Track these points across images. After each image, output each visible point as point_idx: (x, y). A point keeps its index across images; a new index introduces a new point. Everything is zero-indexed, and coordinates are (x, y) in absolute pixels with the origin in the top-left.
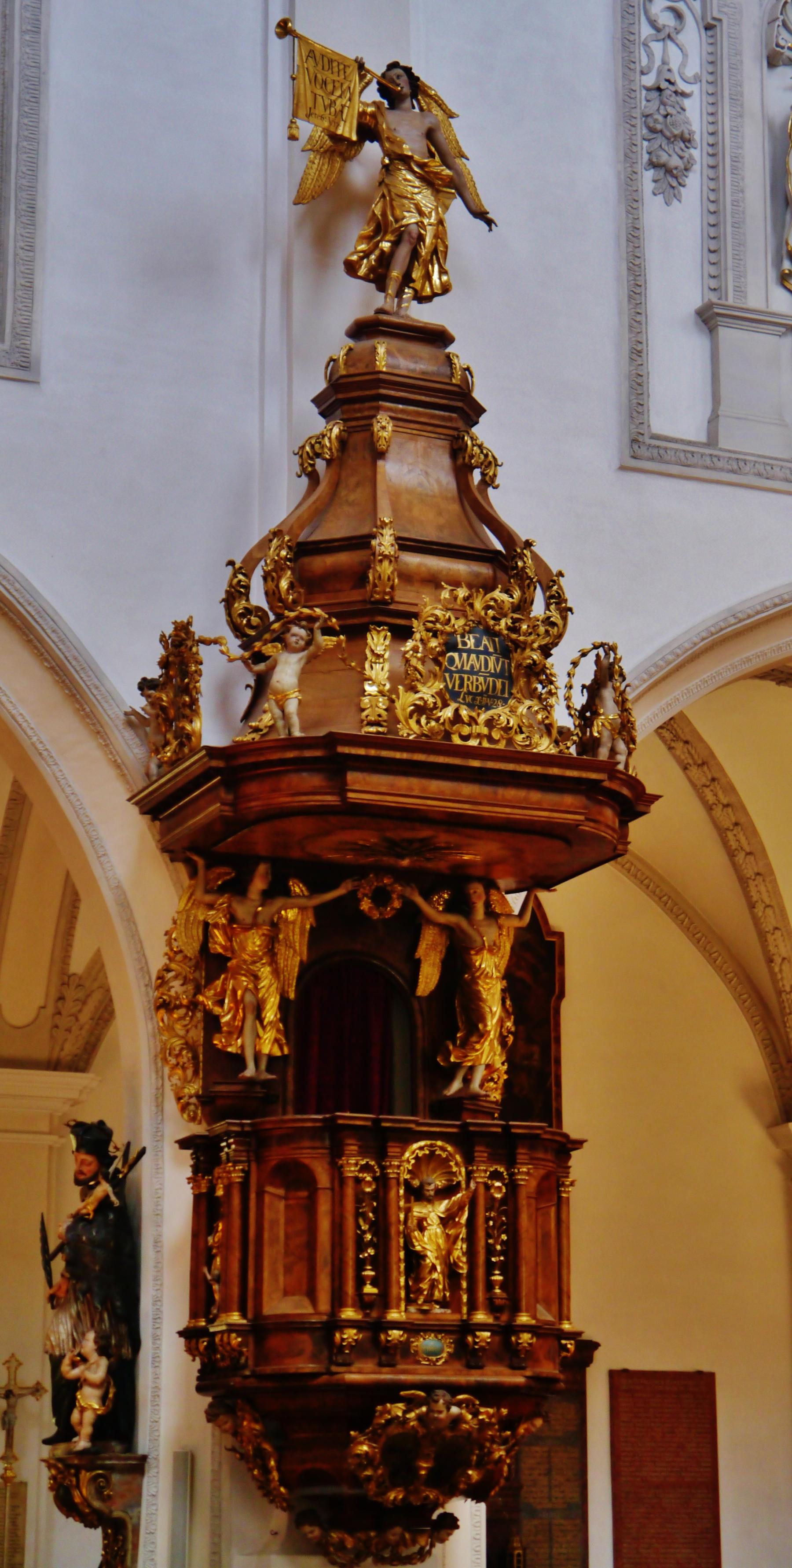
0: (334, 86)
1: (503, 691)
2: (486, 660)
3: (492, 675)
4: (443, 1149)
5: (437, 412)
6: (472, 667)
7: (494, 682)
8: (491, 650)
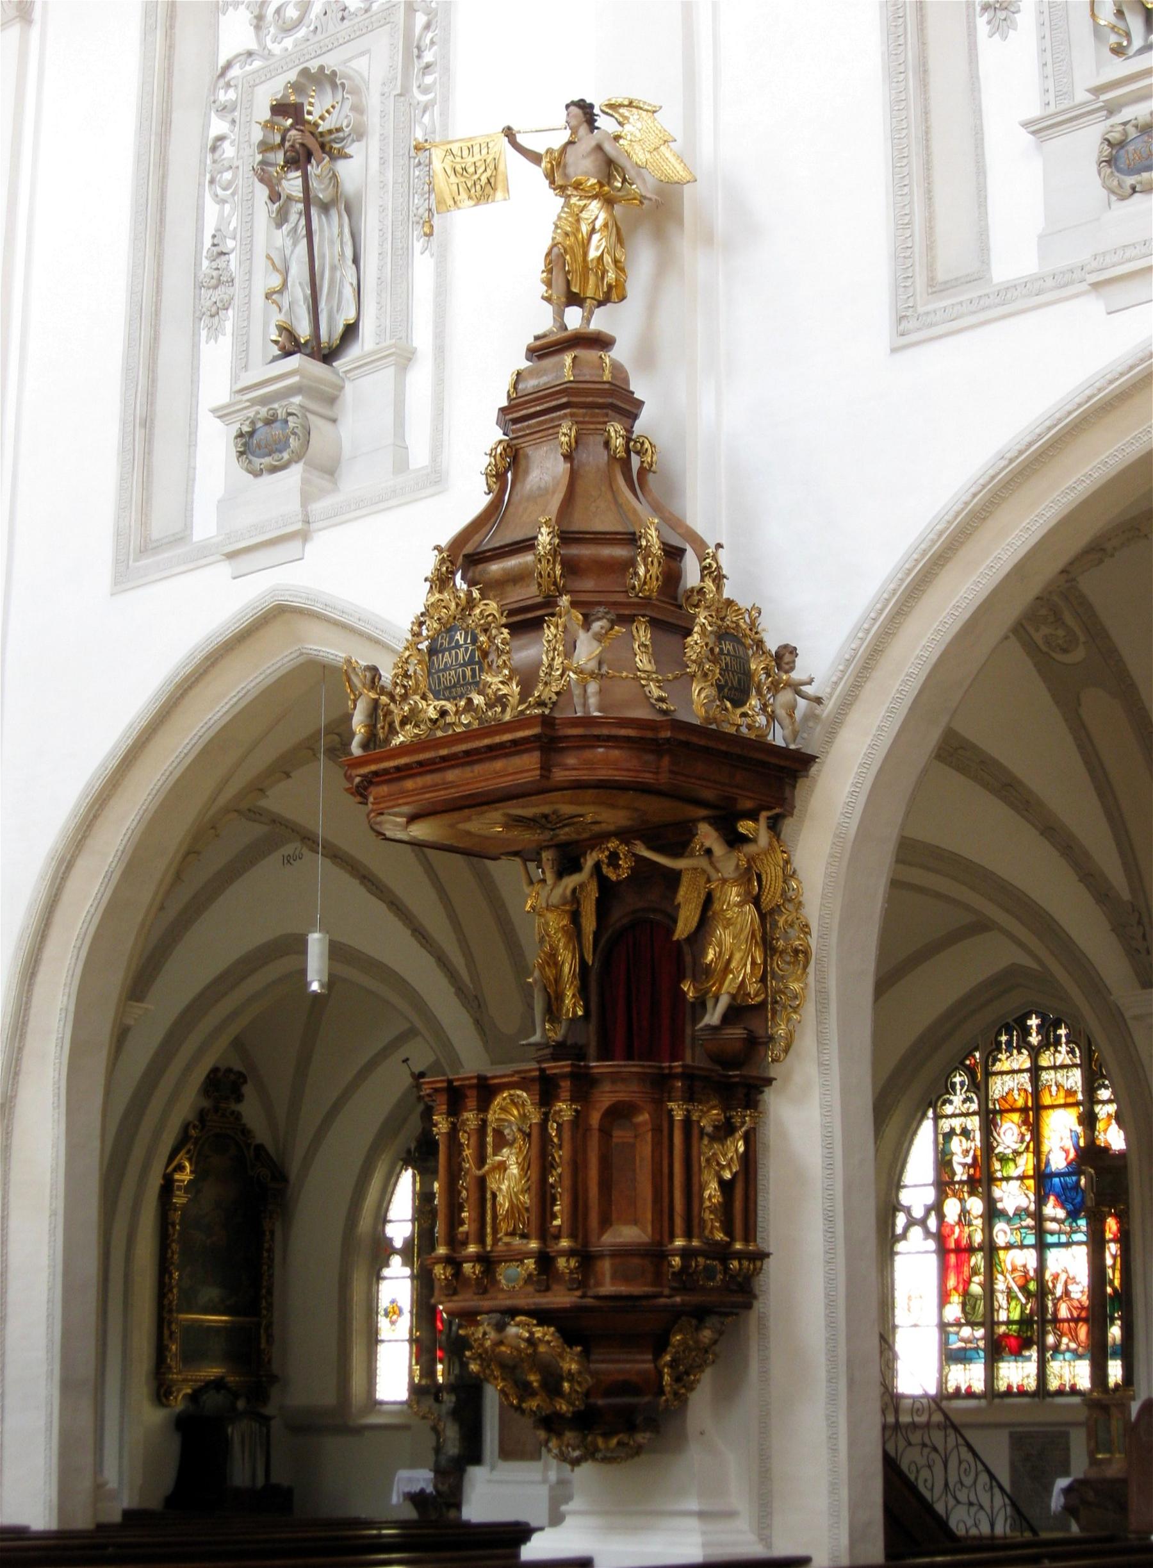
1: (474, 675)
2: (457, 654)
3: (461, 665)
7: (464, 672)
8: (461, 642)
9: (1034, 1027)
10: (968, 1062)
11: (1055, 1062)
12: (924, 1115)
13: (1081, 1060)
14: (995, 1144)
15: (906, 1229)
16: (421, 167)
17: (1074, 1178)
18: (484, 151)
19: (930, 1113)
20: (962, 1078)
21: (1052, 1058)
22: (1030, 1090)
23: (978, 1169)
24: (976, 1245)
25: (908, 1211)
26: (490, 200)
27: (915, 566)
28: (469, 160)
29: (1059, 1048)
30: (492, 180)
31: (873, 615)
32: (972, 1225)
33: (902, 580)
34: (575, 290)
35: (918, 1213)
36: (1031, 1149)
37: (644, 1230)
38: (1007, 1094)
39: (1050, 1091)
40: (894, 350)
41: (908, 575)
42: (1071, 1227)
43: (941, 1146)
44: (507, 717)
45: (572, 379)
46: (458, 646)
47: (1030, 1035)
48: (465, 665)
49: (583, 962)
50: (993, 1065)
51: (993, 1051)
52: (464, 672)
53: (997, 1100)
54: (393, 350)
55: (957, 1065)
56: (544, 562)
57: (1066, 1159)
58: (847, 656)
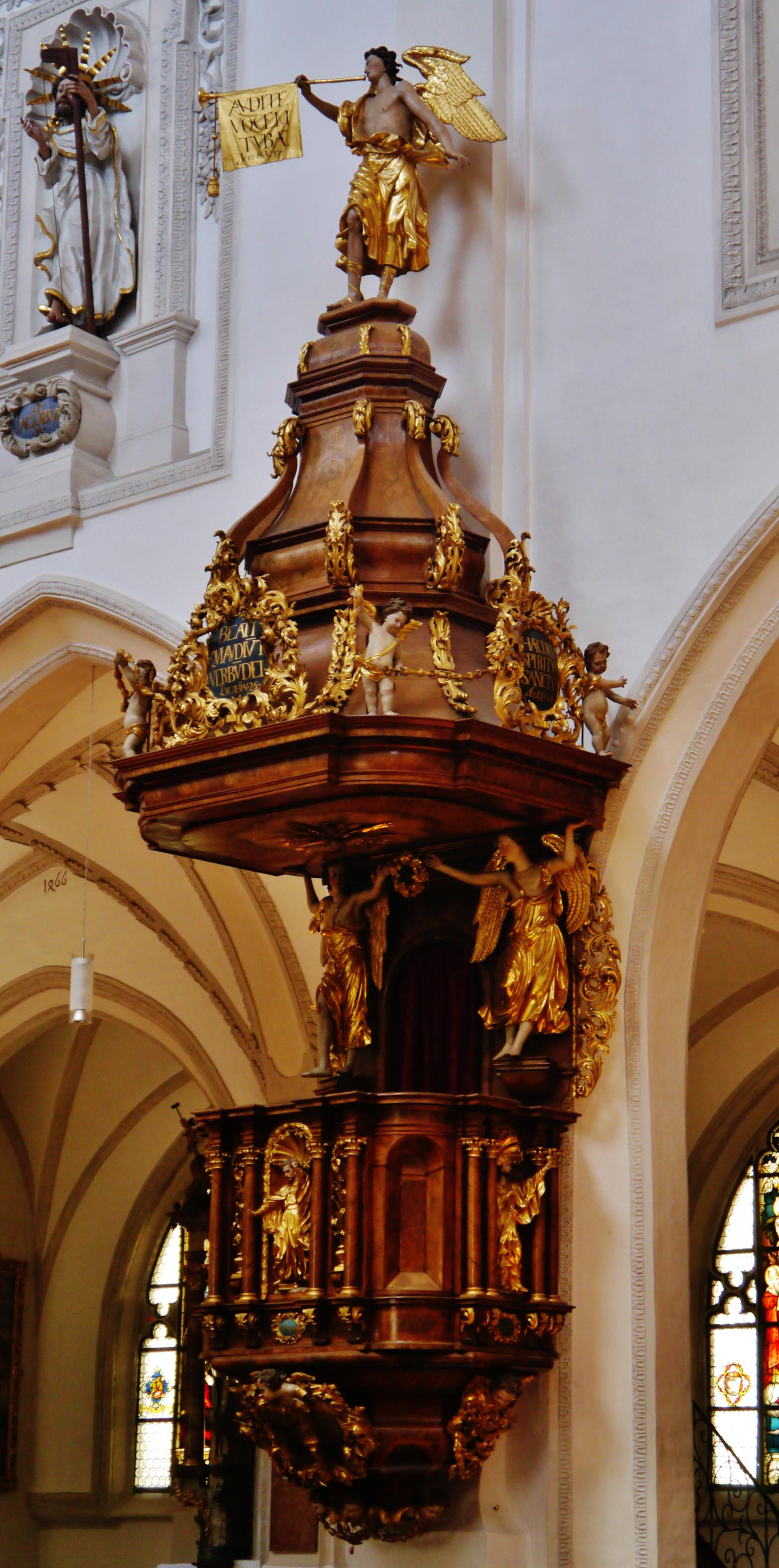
0: (266, 120)
1: (257, 672)
2: (239, 648)
4: (283, 1132)
5: (348, 392)
6: (227, 658)
7: (246, 667)
8: (245, 635)
12: (743, 1176)
15: (724, 1299)
16: (206, 123)
18: (276, 103)
19: (751, 1172)
25: (725, 1278)
26: (281, 157)
27: (738, 559)
28: (260, 113)
30: (284, 136)
31: (692, 612)
33: (724, 574)
34: (373, 256)
35: (737, 1281)
37: (435, 1279)
40: (719, 325)
41: (731, 568)
43: (762, 1208)
44: (293, 716)
45: (368, 352)
46: (241, 640)
48: (248, 660)
49: (371, 987)
52: (246, 667)
54: (173, 323)
56: (335, 550)
58: (663, 657)
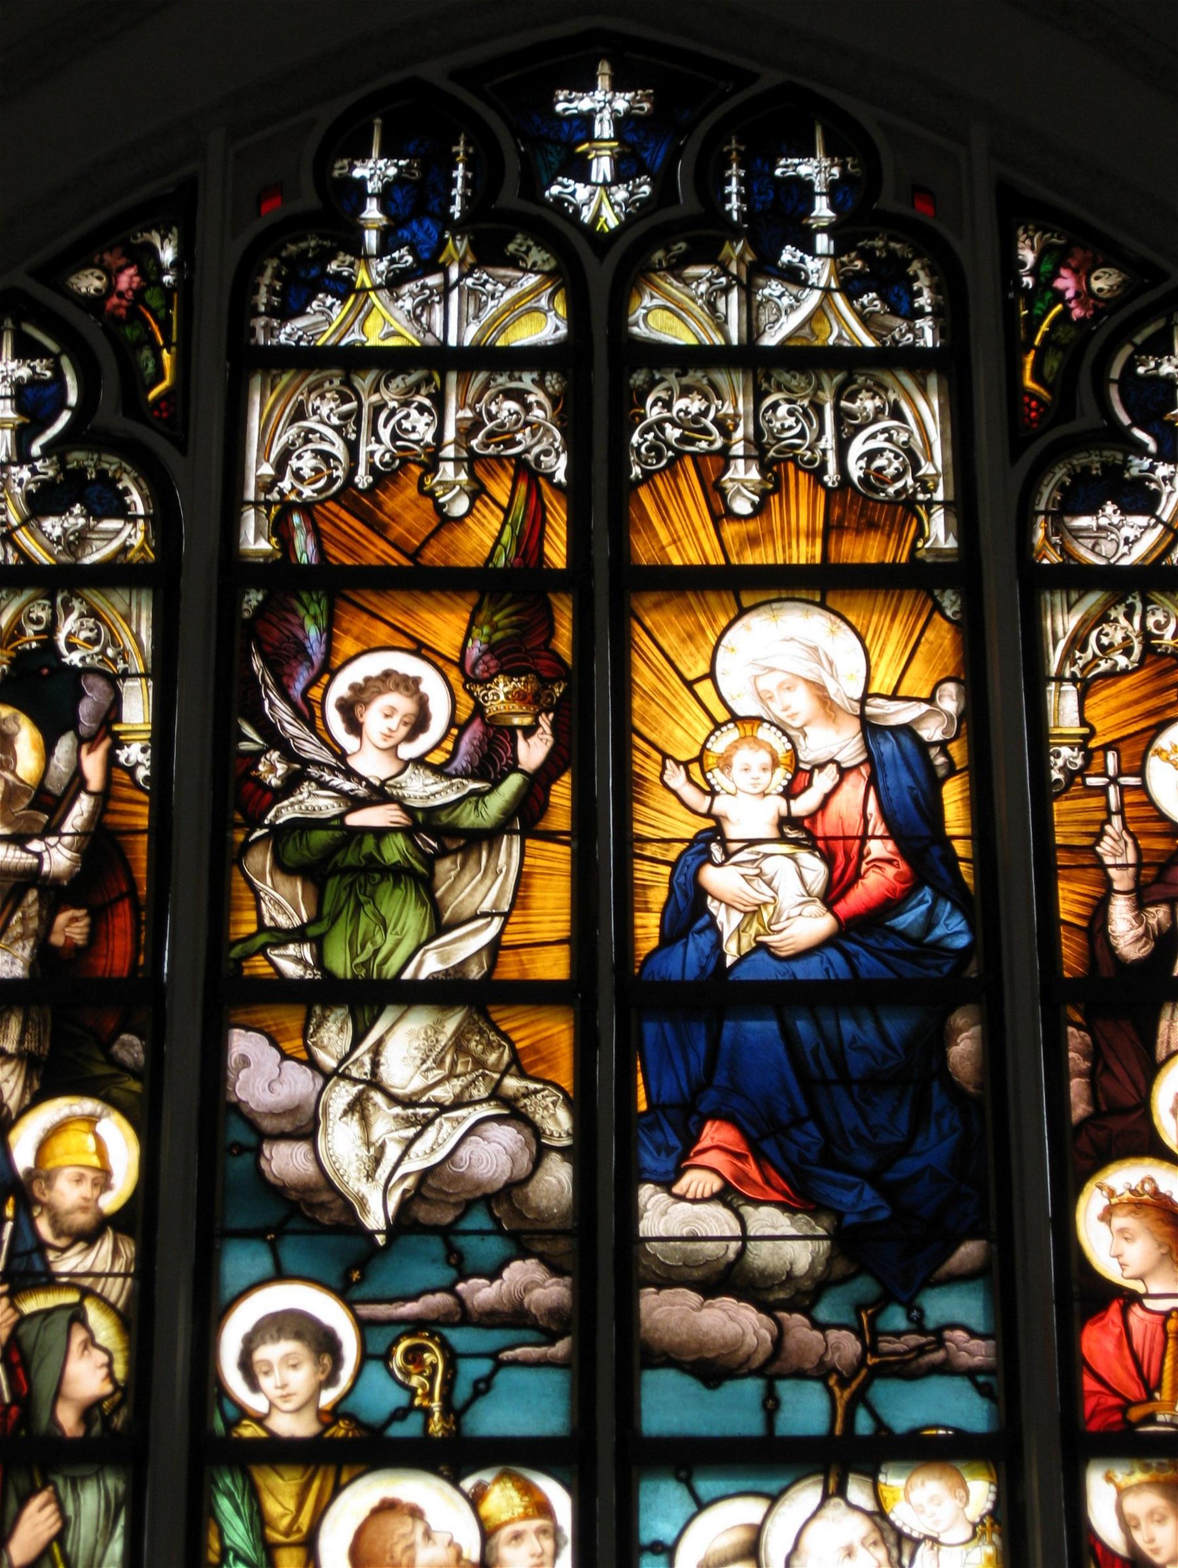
9: (604, 129)
10: (89, 283)
11: (752, 329)
13: (941, 331)
14: (273, 768)
17: (897, 1026)
20: (42, 368)
21: (732, 306)
22: (560, 467)
23: (122, 919)
24: (68, 1418)
29: (789, 255)
32: (48, 1281)
36: (560, 816)
38: (383, 477)
39: (715, 494)
42: (870, 1337)
47: (621, 123)
50: (287, 311)
51: (295, 226)
53: (306, 508)
55: (19, 279)
57: (831, 896)
